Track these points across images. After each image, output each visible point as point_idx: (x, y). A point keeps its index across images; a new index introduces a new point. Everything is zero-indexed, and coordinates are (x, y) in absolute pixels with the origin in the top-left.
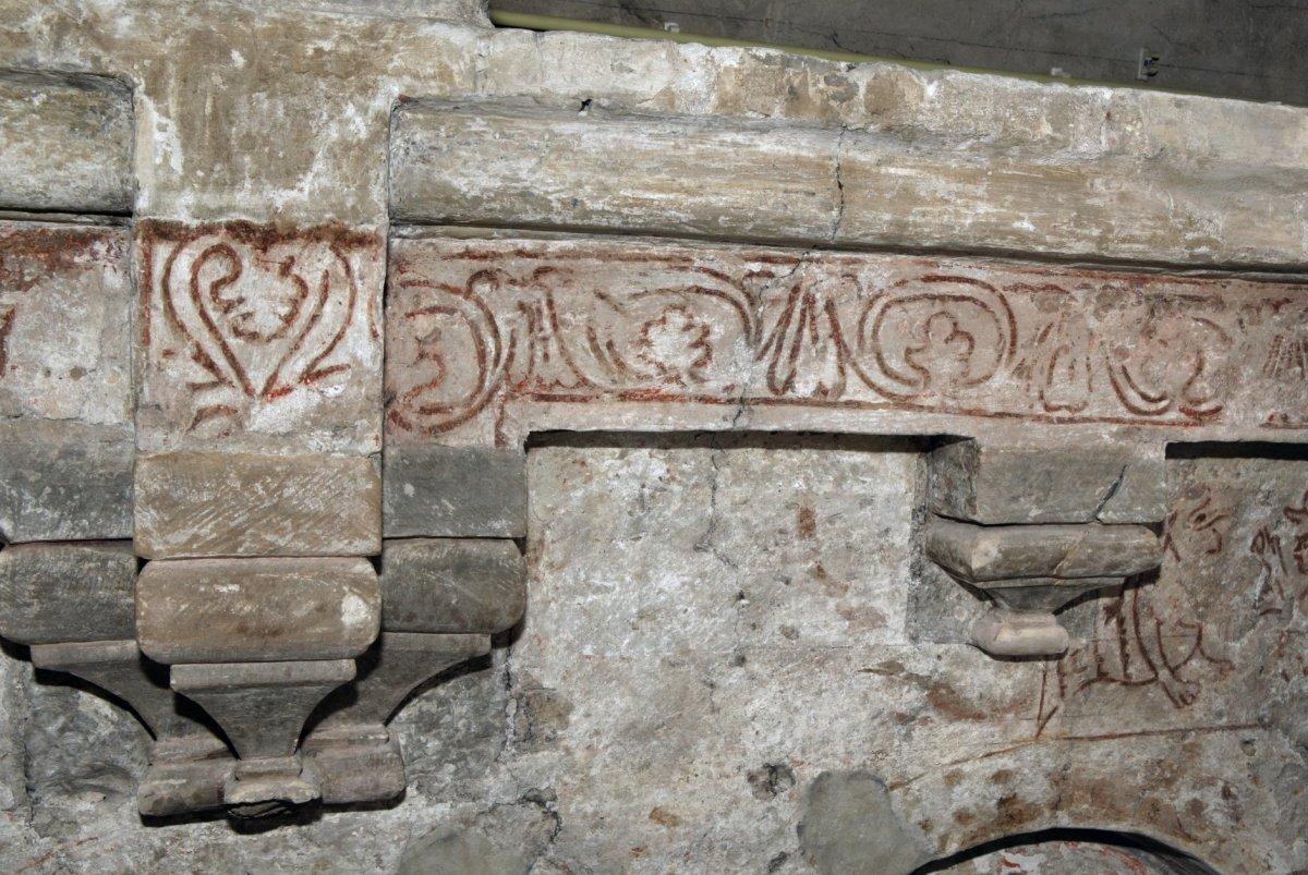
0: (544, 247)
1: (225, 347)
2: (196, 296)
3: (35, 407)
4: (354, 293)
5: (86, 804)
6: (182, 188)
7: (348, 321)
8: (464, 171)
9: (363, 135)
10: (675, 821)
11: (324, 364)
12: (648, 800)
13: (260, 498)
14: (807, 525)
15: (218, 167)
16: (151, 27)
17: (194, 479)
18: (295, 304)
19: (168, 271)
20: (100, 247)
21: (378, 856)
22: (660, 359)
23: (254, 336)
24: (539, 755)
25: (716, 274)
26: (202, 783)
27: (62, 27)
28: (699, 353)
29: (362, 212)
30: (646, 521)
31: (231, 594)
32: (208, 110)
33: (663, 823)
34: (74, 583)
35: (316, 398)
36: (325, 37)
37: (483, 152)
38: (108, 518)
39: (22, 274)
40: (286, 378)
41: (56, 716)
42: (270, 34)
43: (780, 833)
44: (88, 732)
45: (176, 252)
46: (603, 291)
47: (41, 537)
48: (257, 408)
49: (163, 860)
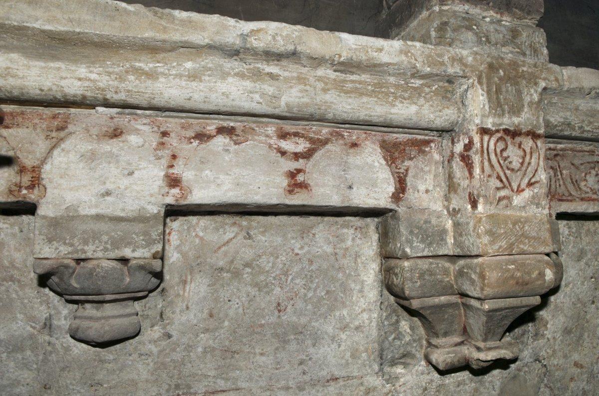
0: (556, 147)
1: (505, 174)
3: (416, 204)
4: (539, 154)
5: (399, 370)
9: (536, 100)
10: (582, 367)
11: (533, 180)
13: (518, 231)
15: (498, 109)
18: (524, 158)
19: (488, 145)
20: (433, 145)
23: (512, 170)
26: (459, 355)
27: (453, 60)
31: (513, 269)
32: (494, 89)
34: (431, 273)
35: (532, 193)
36: (524, 66)
38: (439, 247)
40: (523, 186)
42: (509, 64)
47: (419, 255)
49: (426, 392)
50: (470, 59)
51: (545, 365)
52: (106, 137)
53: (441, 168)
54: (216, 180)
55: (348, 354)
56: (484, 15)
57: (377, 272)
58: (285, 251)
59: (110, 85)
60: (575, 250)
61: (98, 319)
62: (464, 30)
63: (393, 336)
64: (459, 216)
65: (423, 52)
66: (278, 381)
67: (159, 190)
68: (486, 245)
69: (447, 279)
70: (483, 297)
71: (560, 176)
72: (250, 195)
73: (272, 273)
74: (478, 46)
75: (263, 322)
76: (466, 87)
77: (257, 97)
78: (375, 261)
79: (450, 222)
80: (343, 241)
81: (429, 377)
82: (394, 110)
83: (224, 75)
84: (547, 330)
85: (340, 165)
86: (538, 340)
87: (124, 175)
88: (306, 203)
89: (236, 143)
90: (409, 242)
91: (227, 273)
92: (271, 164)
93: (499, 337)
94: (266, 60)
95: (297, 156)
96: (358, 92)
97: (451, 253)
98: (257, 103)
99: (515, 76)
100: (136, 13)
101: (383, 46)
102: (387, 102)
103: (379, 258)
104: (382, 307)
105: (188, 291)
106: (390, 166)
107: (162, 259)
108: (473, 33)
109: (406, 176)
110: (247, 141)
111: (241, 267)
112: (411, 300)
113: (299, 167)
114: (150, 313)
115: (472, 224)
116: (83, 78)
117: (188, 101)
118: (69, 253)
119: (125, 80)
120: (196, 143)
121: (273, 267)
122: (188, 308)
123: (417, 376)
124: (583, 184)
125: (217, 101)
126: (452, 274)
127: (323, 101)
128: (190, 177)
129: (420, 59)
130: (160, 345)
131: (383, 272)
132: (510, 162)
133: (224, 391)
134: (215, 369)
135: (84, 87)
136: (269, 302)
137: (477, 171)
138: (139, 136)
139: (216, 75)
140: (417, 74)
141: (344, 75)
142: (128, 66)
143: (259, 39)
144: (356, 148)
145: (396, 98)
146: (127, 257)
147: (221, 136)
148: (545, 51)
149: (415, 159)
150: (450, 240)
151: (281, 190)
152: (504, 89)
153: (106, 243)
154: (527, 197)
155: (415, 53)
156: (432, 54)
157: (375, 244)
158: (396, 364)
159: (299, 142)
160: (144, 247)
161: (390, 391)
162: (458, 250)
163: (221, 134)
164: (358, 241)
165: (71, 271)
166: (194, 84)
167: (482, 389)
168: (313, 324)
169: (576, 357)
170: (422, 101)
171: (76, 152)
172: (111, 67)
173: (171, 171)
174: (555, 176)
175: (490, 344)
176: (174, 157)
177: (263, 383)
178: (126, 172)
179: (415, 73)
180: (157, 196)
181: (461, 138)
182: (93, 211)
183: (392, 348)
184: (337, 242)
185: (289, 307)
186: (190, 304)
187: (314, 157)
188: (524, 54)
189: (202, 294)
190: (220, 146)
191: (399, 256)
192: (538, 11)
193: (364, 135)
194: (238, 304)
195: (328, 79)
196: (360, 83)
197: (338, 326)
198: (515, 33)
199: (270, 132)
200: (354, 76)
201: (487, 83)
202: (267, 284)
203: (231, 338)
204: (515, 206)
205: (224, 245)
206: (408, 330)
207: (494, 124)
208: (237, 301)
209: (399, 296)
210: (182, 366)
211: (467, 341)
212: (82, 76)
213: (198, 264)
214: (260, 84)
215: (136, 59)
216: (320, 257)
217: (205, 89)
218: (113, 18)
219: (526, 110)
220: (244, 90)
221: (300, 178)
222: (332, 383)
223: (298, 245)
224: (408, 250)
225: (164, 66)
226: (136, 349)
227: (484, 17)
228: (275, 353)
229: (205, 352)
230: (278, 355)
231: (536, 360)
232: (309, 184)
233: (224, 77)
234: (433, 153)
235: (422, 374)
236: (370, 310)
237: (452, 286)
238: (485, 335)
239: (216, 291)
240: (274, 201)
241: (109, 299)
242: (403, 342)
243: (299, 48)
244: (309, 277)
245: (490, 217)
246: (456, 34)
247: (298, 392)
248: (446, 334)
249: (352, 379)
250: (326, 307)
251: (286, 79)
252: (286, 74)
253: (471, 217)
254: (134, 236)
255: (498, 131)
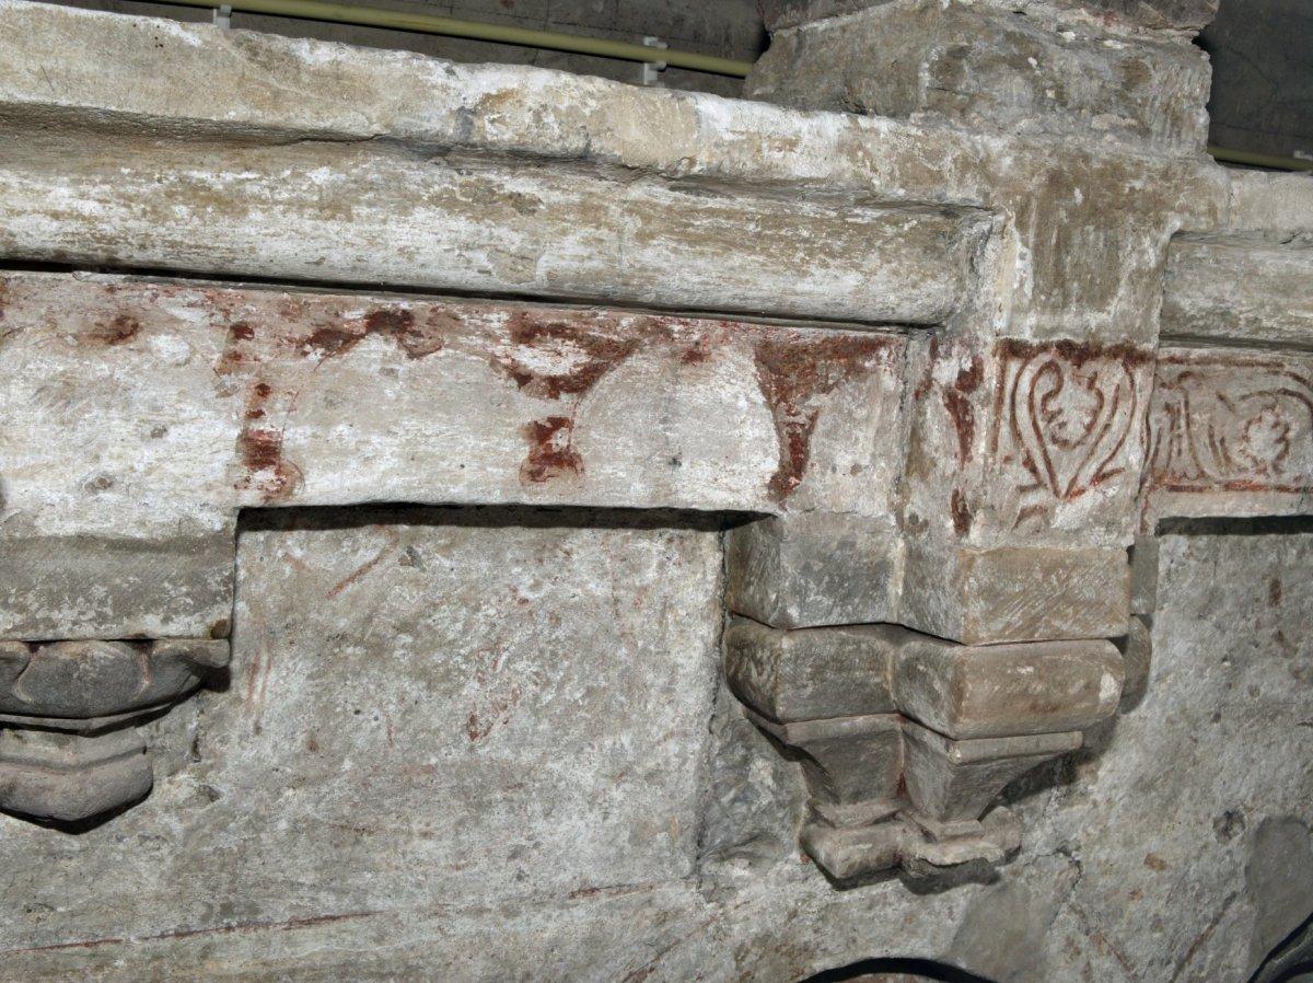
0: (1188, 354)
1: (1045, 453)
2: (1031, 407)
3: (826, 502)
4: (1135, 404)
5: (738, 870)
6: (1029, 310)
7: (1128, 430)
8: (1189, 293)
9: (1153, 264)
10: (1162, 866)
11: (1109, 467)
12: (1145, 847)
13: (1053, 589)
14: (1275, 595)
15: (1055, 292)
16: (1023, 166)
17: (1011, 572)
18: (1095, 413)
19: (1016, 385)
20: (883, 353)
21: (950, 908)
22: (1255, 454)
23: (1065, 443)
24: (1075, 808)
25: (1297, 378)
26: (882, 846)
27: (965, 165)
28: (1281, 447)
29: (1141, 334)
30: (1171, 594)
32: (1054, 241)
33: (1153, 867)
34: (840, 664)
35: (1100, 497)
36: (1137, 177)
37: (1201, 276)
38: (866, 604)
39: (827, 376)
40: (1083, 481)
41: (731, 788)
42: (1101, 174)
43: (1233, 874)
44: (752, 802)
45: (1025, 364)
46: (1222, 393)
47: (818, 623)
48: (1060, 507)
49: (794, 921)
50: (1008, 161)
51: (1078, 862)
52: (97, 341)
53: (896, 411)
54: (362, 448)
55: (626, 835)
56: (1062, 20)
57: (710, 646)
58: (496, 593)
59: (129, 229)
60: (1195, 594)
61: (64, 769)
62: (1004, 68)
63: (732, 794)
64: (924, 536)
65: (894, 147)
66: (458, 895)
67: (227, 475)
68: (975, 621)
69: (877, 680)
70: (952, 735)
71: (1183, 428)
72: (439, 485)
73: (462, 647)
74: (1032, 115)
75: (433, 761)
76: (986, 227)
77: (481, 258)
78: (709, 618)
79: (901, 544)
80: (635, 569)
81: (806, 888)
82: (804, 286)
83: (406, 203)
84: (1094, 783)
85: (656, 407)
86: (1072, 805)
87: (143, 438)
88: (568, 501)
89: (412, 355)
90: (799, 592)
91: (356, 646)
92: (494, 407)
93: (978, 811)
94: (509, 166)
95: (555, 386)
96: (726, 242)
97: (894, 619)
98: (479, 271)
99: (1110, 205)
100: (205, 54)
101: (797, 133)
102: (789, 265)
103: (719, 611)
104: (713, 727)
105: (259, 689)
106: (773, 408)
107: (230, 637)
108: (1027, 78)
109: (809, 432)
110: (439, 349)
111: (391, 632)
112: (787, 725)
113: (558, 414)
114: (168, 742)
115: (950, 566)
116: (63, 213)
117: (314, 267)
118: (15, 629)
119: (166, 218)
120: (316, 354)
121: (465, 632)
122: (258, 730)
123: (778, 884)
124: (1235, 449)
125: (383, 263)
126: (889, 668)
127: (638, 266)
128: (302, 441)
129: (884, 168)
130: (191, 816)
131: (724, 645)
132: (1063, 425)
133: (333, 918)
134: (316, 869)
135: (66, 234)
136: (452, 714)
137: (980, 446)
138: (178, 337)
139: (387, 203)
140: (868, 199)
141: (693, 198)
142: (172, 178)
143: (501, 120)
144: (698, 364)
145: (811, 253)
146: (150, 636)
147: (376, 335)
148: (1203, 118)
149: (835, 390)
150: (895, 589)
151: (512, 472)
152: (1077, 240)
153: (102, 603)
154: (1088, 506)
155: (874, 152)
156: (916, 152)
157: (711, 577)
158: (731, 856)
159: (564, 350)
160: (188, 611)
161: (713, 918)
162: (912, 616)
163: (377, 330)
164: (673, 571)
165: (19, 668)
166: (332, 227)
167: (924, 916)
168: (550, 765)
169: (1152, 844)
170: (873, 260)
171: (26, 379)
172: (133, 183)
173: (256, 426)
174: (1172, 428)
175: (956, 825)
176: (263, 390)
177: (424, 901)
178: (148, 429)
179: (869, 198)
180: (222, 489)
181: (955, 350)
182: (71, 528)
183: (726, 822)
184: (623, 573)
185: (497, 727)
186: (263, 722)
187: (596, 387)
188: (1144, 132)
189: (292, 699)
190: (375, 360)
191: (770, 621)
192: (1202, 8)
193: (720, 331)
194: (376, 719)
195: (654, 206)
196: (729, 215)
197: (608, 770)
198: (1133, 73)
199: (495, 325)
200: (719, 199)
201: (1039, 226)
202: (448, 672)
203: (356, 799)
204: (1057, 529)
205: (352, 579)
206: (769, 781)
207: (1038, 330)
208: (376, 712)
209: (763, 719)
210: (240, 863)
211: (904, 812)
212: (62, 208)
213: (287, 627)
214: (489, 226)
215: (192, 162)
216: (577, 607)
217: (358, 241)
218: (147, 68)
219: (1121, 292)
220: (451, 241)
221: (559, 440)
222: (582, 900)
223: (528, 580)
224: (793, 612)
225: (261, 179)
226: (133, 825)
227: (1061, 29)
228: (457, 833)
229: (294, 831)
230: (463, 837)
231: (1058, 851)
232: (579, 456)
233: (406, 208)
234: (882, 373)
235: (791, 880)
236: (685, 734)
237: (886, 696)
238: (947, 807)
239: (328, 689)
240: (496, 497)
241: (98, 726)
242: (754, 808)
243: (596, 146)
244: (548, 655)
245: (996, 555)
246: (982, 78)
247: (502, 919)
248: (856, 797)
249: (629, 891)
250: (583, 725)
251: (555, 212)
252: (556, 197)
253: (950, 549)
254: (166, 584)
255: (1044, 348)
